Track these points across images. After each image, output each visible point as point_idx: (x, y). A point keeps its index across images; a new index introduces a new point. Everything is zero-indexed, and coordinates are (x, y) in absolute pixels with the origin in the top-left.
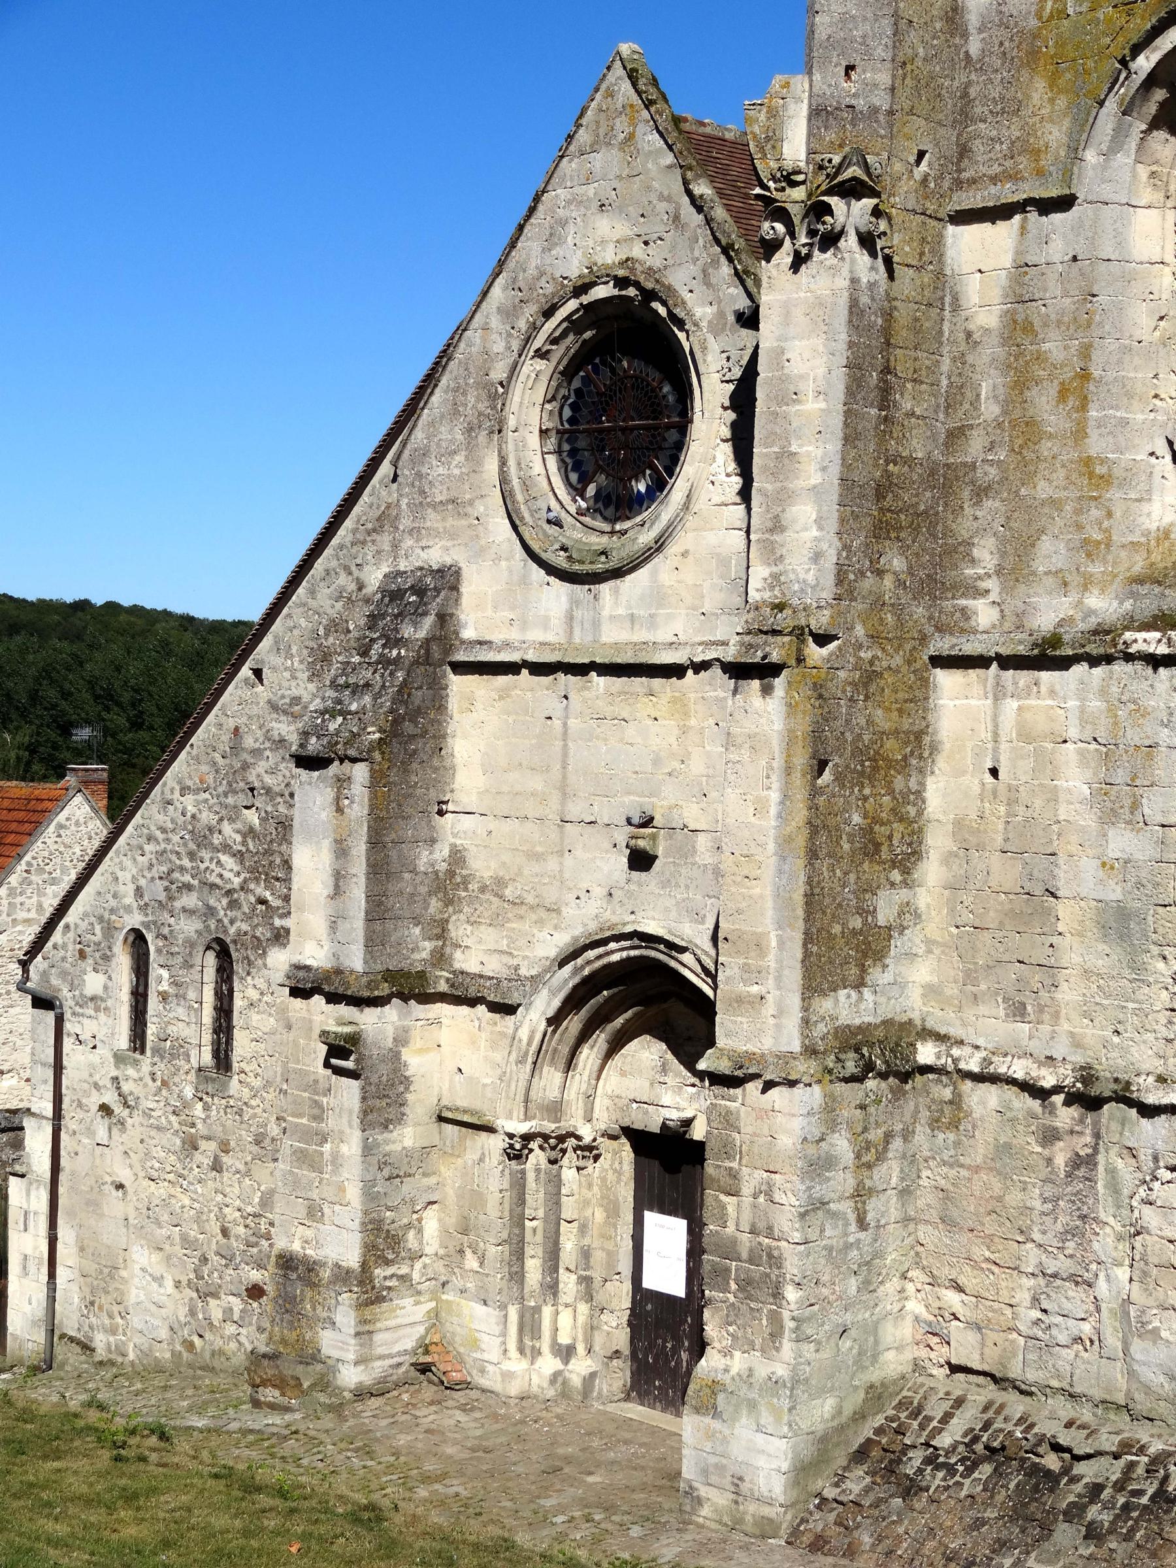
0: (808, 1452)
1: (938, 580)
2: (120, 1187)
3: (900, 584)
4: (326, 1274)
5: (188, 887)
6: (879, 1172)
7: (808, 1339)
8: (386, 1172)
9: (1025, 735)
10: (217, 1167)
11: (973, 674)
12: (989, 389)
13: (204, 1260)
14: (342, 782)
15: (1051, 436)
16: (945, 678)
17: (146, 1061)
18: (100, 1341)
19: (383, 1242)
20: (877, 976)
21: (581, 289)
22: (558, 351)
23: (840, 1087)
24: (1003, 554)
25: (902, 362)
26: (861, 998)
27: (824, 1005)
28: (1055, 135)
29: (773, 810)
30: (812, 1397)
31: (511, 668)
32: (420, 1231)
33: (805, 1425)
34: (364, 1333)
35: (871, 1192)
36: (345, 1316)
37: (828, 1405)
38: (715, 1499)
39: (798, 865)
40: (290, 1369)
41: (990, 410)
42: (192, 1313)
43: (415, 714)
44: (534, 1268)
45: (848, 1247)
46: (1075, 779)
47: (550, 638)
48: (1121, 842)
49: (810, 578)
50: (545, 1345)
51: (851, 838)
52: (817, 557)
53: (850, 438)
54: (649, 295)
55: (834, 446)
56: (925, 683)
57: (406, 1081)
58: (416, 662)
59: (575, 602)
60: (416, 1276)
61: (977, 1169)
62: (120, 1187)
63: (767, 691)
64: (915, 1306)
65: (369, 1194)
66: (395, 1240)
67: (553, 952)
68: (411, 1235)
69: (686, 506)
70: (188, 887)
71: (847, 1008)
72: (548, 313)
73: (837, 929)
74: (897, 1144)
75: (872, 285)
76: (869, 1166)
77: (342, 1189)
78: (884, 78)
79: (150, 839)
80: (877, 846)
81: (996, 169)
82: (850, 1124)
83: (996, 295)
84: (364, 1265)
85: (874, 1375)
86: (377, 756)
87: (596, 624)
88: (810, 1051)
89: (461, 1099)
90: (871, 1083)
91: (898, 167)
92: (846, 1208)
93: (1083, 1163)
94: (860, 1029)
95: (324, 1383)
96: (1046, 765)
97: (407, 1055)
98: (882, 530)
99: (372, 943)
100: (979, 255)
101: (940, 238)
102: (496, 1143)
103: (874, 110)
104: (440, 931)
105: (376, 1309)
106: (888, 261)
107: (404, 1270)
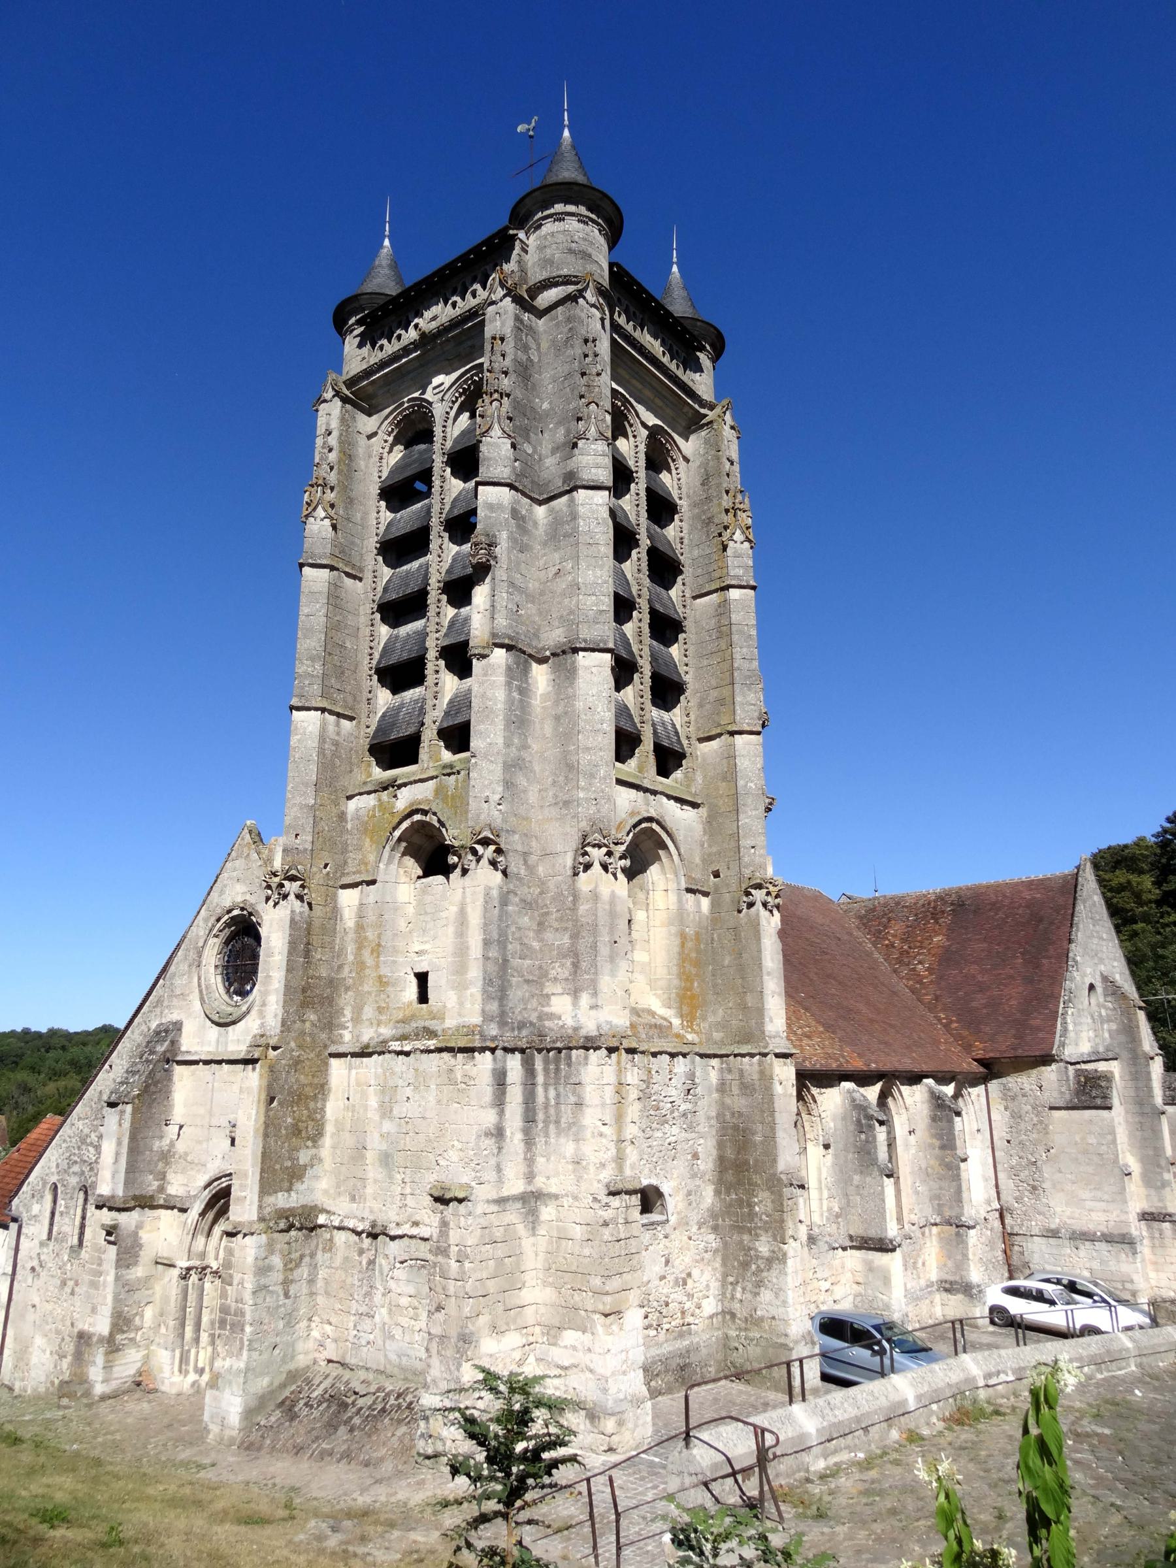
0: (253, 1404)
1: (330, 1024)
2: (34, 1306)
3: (313, 1025)
4: (95, 1339)
5: (76, 1162)
6: (297, 1274)
7: (255, 1350)
8: (126, 1288)
9: (358, 1084)
10: (72, 1293)
11: (343, 1059)
12: (350, 948)
13: (63, 1339)
14: (122, 1112)
16: (334, 1062)
17: (51, 1244)
18: (17, 1386)
19: (122, 1322)
20: (298, 1186)
21: (229, 912)
22: (222, 935)
23: (276, 1235)
25: (315, 941)
26: (290, 1196)
27: (270, 1200)
28: (372, 858)
30: (256, 1377)
31: (195, 1062)
32: (142, 1316)
33: (252, 1390)
34: (108, 1367)
35: (292, 1281)
36: (100, 1359)
37: (265, 1381)
38: (214, 1429)
39: (260, 1141)
40: (73, 1388)
41: (351, 958)
42: (56, 1367)
43: (156, 1084)
44: (189, 1330)
45: (279, 1306)
46: (373, 1102)
47: (211, 1049)
48: (388, 1126)
50: (191, 1368)
51: (286, 1128)
52: (276, 1016)
53: (290, 970)
54: (251, 914)
55: (283, 973)
56: (327, 1064)
57: (140, 1246)
58: (159, 1061)
59: (220, 1034)
60: (138, 1338)
61: (337, 1269)
62: (34, 1306)
63: (254, 1069)
64: (315, 1334)
65: (117, 1299)
66: (128, 1321)
67: (202, 1183)
68: (137, 1318)
70: (76, 1162)
71: (281, 1200)
72: (218, 920)
73: (278, 1167)
74: (307, 1259)
75: (301, 913)
76: (291, 1270)
77: (105, 1297)
78: (310, 838)
79: (65, 1141)
80: (300, 1132)
82: (281, 1252)
83: (353, 915)
84: (111, 1334)
85: (292, 1366)
86: (136, 1101)
87: (227, 1043)
88: (262, 1219)
89: (164, 1253)
90: (293, 1233)
91: (314, 869)
92: (279, 1289)
93: (371, 1262)
94: (289, 1209)
95: (87, 1393)
96: (364, 1096)
97: (141, 1233)
98: (304, 1005)
99: (127, 1183)
100: (348, 899)
101: (335, 895)
102: (175, 1272)
104: (162, 1177)
105: (116, 1355)
106: (310, 904)
107: (132, 1335)
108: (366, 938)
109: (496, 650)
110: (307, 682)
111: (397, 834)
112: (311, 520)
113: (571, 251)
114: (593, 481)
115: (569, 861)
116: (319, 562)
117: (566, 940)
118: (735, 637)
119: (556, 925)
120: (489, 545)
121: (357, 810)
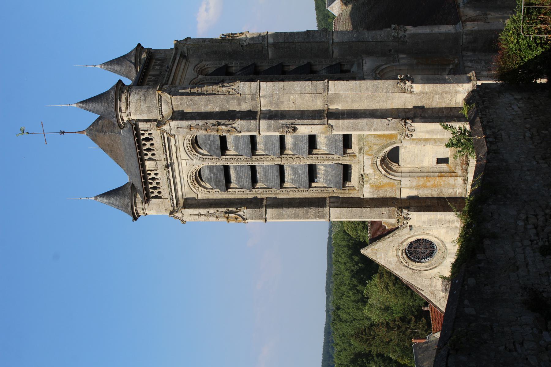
3: (456, 203)
41: (429, 191)
69: (437, 238)
108: (422, 185)
111: (384, 172)
112: (244, 217)
113: (145, 100)
115: (408, 96)
118: (290, 40)
119: (431, 100)
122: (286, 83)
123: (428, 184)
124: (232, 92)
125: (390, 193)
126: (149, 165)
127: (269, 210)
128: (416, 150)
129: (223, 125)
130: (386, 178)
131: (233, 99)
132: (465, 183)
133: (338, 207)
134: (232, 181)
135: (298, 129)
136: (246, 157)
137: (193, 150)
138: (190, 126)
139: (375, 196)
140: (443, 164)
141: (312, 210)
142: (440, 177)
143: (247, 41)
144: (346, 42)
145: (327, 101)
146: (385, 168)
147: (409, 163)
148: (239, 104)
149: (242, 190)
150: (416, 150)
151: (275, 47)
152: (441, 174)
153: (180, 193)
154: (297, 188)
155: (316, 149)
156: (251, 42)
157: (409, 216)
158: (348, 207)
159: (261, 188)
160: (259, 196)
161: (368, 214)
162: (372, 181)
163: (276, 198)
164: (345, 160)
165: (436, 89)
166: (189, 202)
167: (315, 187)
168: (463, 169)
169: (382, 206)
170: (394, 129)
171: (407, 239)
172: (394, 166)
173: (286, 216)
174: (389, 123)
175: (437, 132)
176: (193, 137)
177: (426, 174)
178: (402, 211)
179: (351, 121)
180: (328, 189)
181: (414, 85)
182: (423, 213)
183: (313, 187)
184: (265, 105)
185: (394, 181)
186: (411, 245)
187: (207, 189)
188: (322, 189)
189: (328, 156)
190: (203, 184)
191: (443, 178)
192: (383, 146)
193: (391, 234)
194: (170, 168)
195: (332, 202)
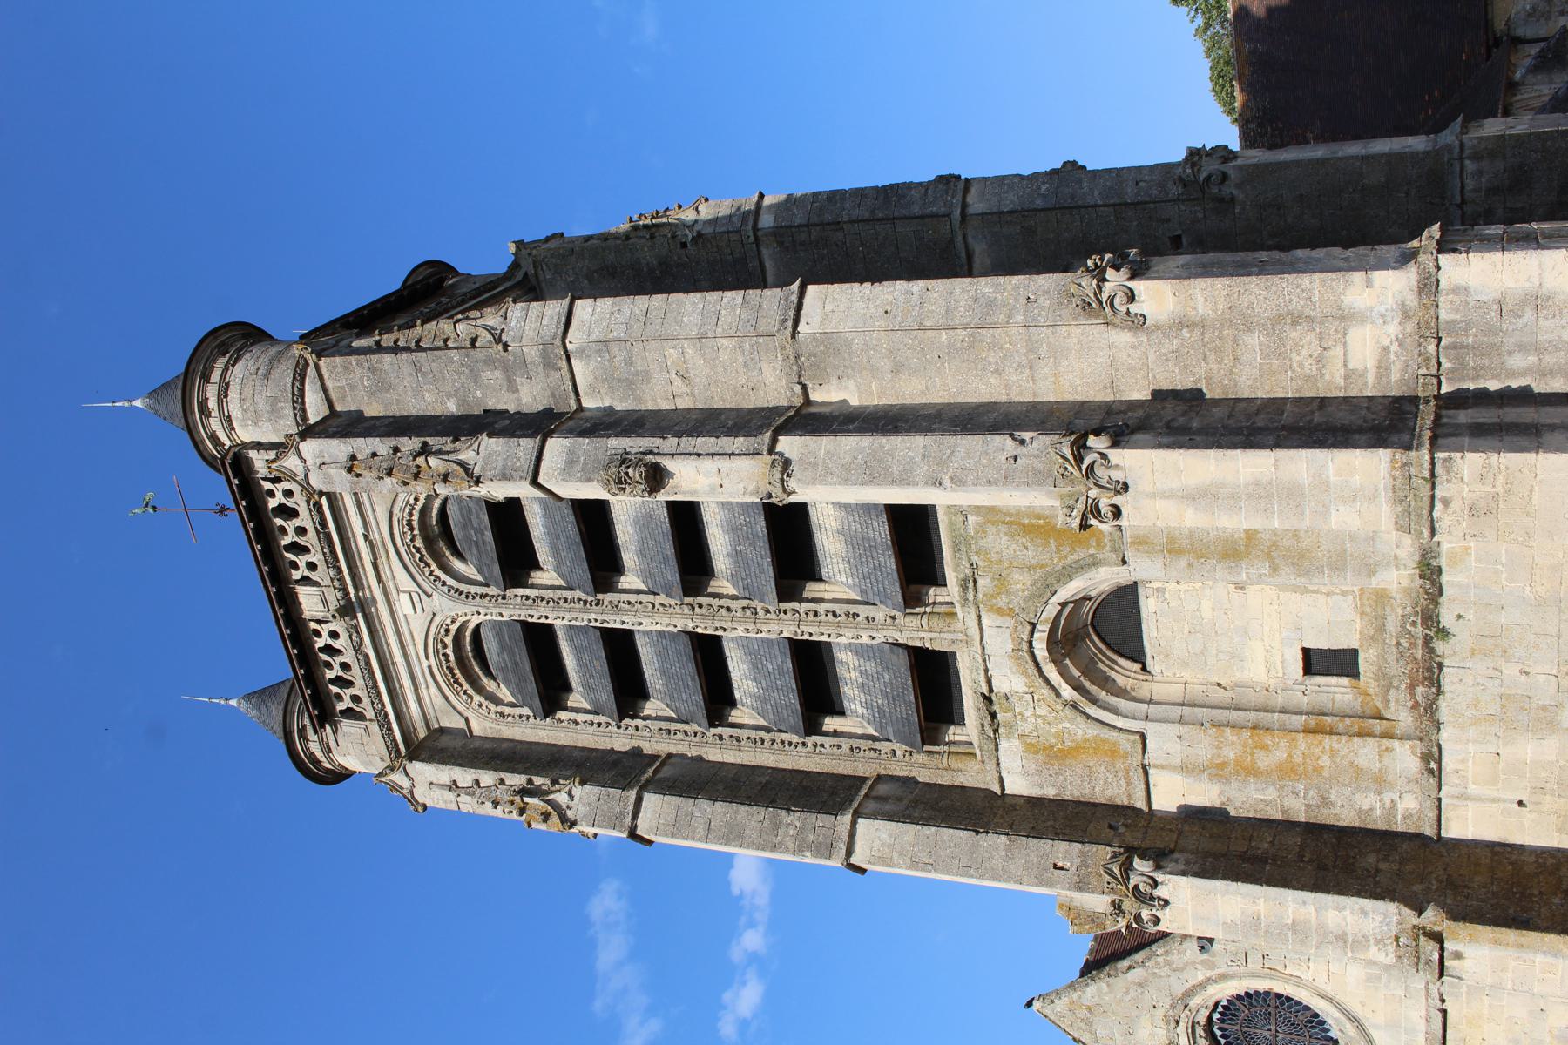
3: (1386, 859)
15: (1290, 756)
24: (1367, 789)
29: (1551, 960)
41: (1271, 793)
46: (1528, 749)
49: (1379, 918)
63: (1458, 956)
69: (1330, 1000)
75: (1187, 863)
81: (1123, 782)
103: (1082, 852)
108: (1238, 762)
109: (779, 448)
110: (811, 838)
111: (1067, 692)
112: (570, 814)
113: (267, 375)
114: (559, 322)
115: (1123, 338)
116: (631, 808)
117: (1253, 340)
118: (828, 217)
120: (623, 462)
121: (1026, 774)
122: (658, 300)
123: (1264, 761)
124: (485, 337)
125: (1109, 786)
126: (310, 602)
127: (651, 800)
128: (1206, 605)
129: (440, 452)
130: (1080, 719)
131: (489, 361)
132: (1431, 771)
133: (890, 817)
134: (574, 685)
135: (671, 475)
136: (584, 596)
137: (430, 561)
138: (353, 457)
139: (1050, 792)
140: (1333, 680)
141: (794, 819)
142: (1313, 732)
143: (697, 228)
144: (1011, 212)
145: (801, 371)
146: (1077, 673)
147: (1184, 664)
148: (513, 388)
149: (597, 719)
150: (1206, 605)
151: (780, 244)
152: (1320, 724)
153: (414, 707)
154: (768, 730)
155: (821, 580)
156: (709, 230)
157: (1160, 892)
158: (927, 822)
159: (658, 718)
160: (648, 748)
161: (997, 861)
162: (1026, 728)
163: (700, 759)
164: (918, 631)
165: (1244, 301)
166: (445, 741)
167: (835, 734)
168: (1416, 706)
169: (1057, 835)
170: (1038, 478)
171: (1202, 986)
172: (1124, 672)
173: (701, 831)
174: (1021, 450)
175: (1234, 497)
176: (424, 512)
177: (1248, 716)
178: (1127, 867)
179: (866, 442)
180: (878, 745)
181: (1138, 286)
182: (1218, 884)
183: (826, 734)
184: (593, 389)
185: (1114, 735)
186: (1229, 1010)
187: (497, 701)
188: (855, 743)
189: (853, 609)
190: (490, 685)
191: (1328, 741)
192: (1048, 575)
193: (1139, 956)
194: (359, 615)
195: (879, 798)
